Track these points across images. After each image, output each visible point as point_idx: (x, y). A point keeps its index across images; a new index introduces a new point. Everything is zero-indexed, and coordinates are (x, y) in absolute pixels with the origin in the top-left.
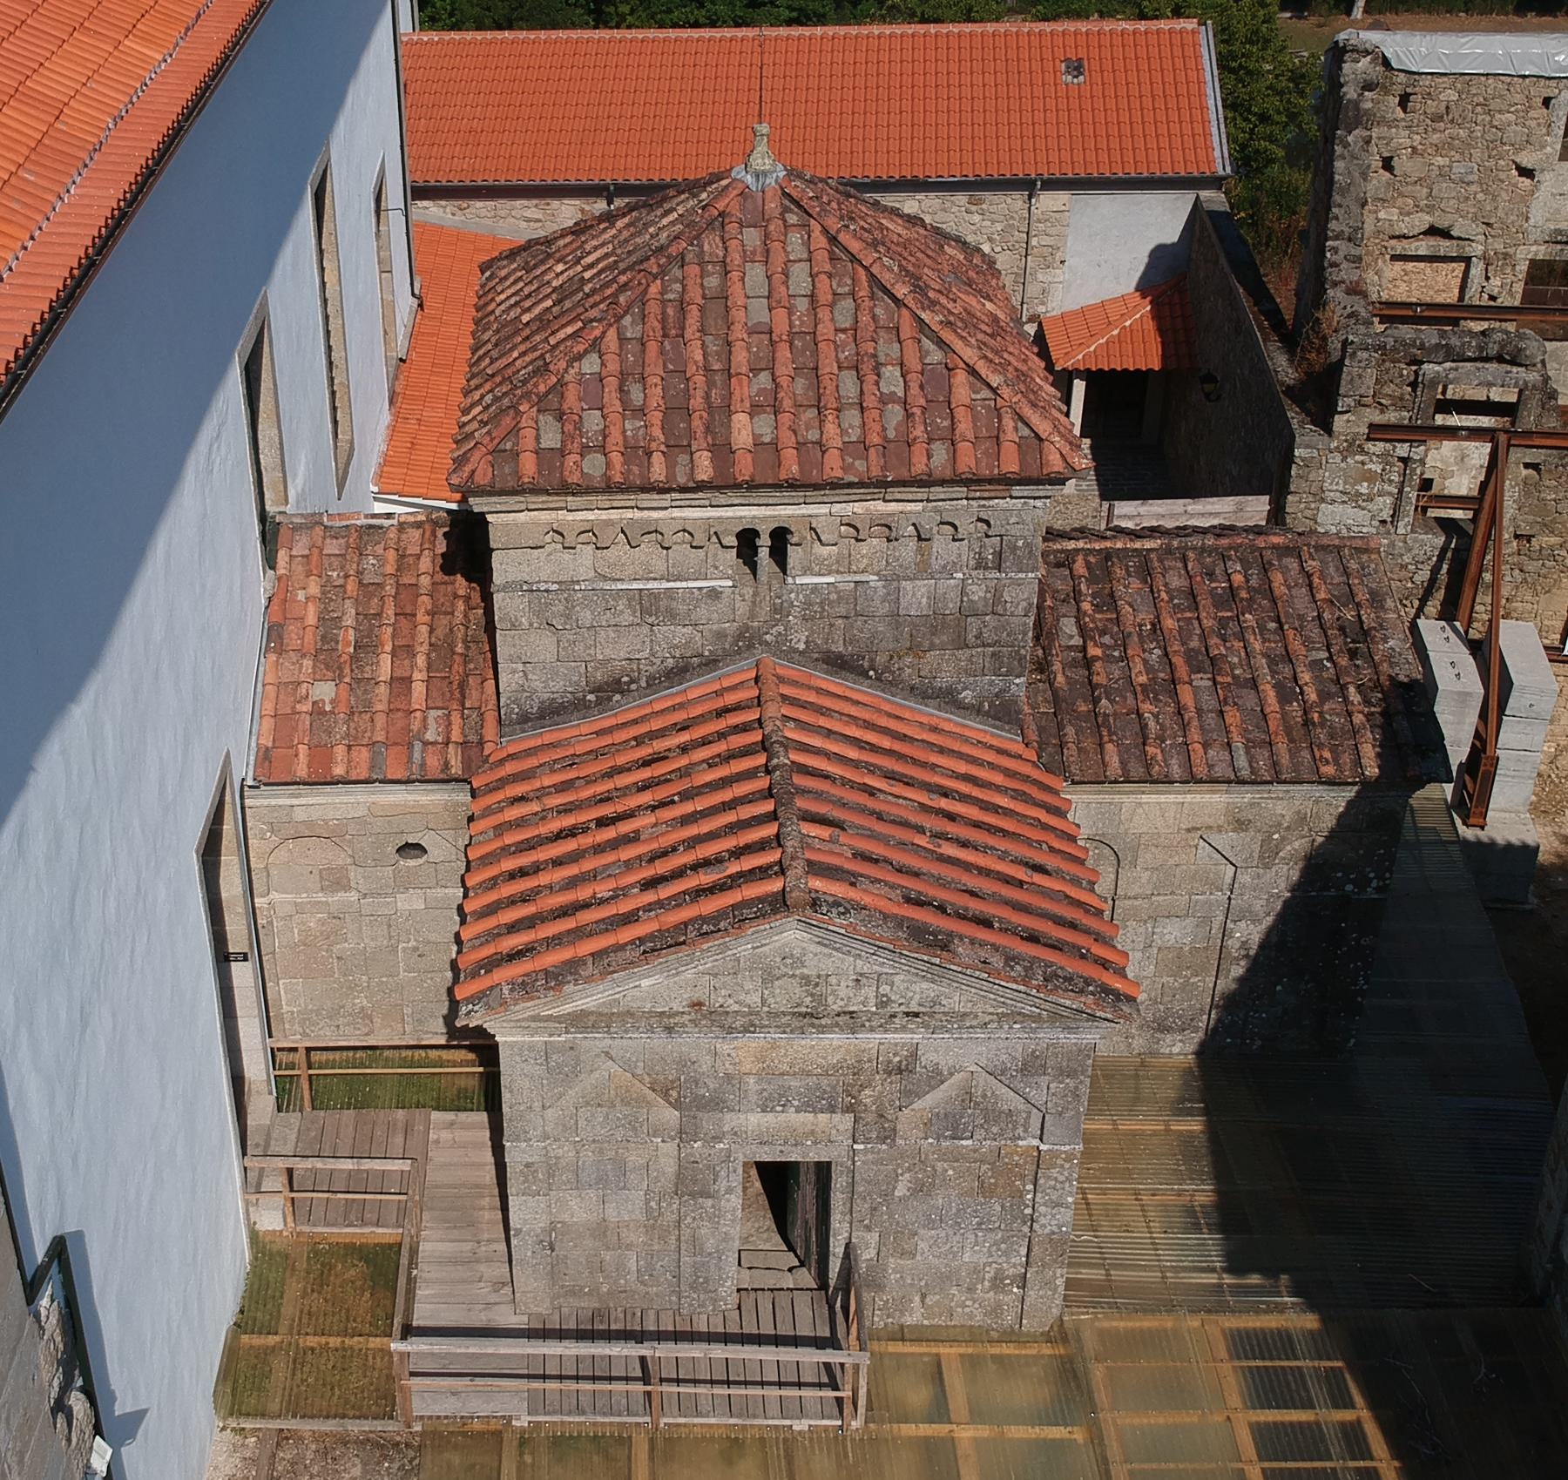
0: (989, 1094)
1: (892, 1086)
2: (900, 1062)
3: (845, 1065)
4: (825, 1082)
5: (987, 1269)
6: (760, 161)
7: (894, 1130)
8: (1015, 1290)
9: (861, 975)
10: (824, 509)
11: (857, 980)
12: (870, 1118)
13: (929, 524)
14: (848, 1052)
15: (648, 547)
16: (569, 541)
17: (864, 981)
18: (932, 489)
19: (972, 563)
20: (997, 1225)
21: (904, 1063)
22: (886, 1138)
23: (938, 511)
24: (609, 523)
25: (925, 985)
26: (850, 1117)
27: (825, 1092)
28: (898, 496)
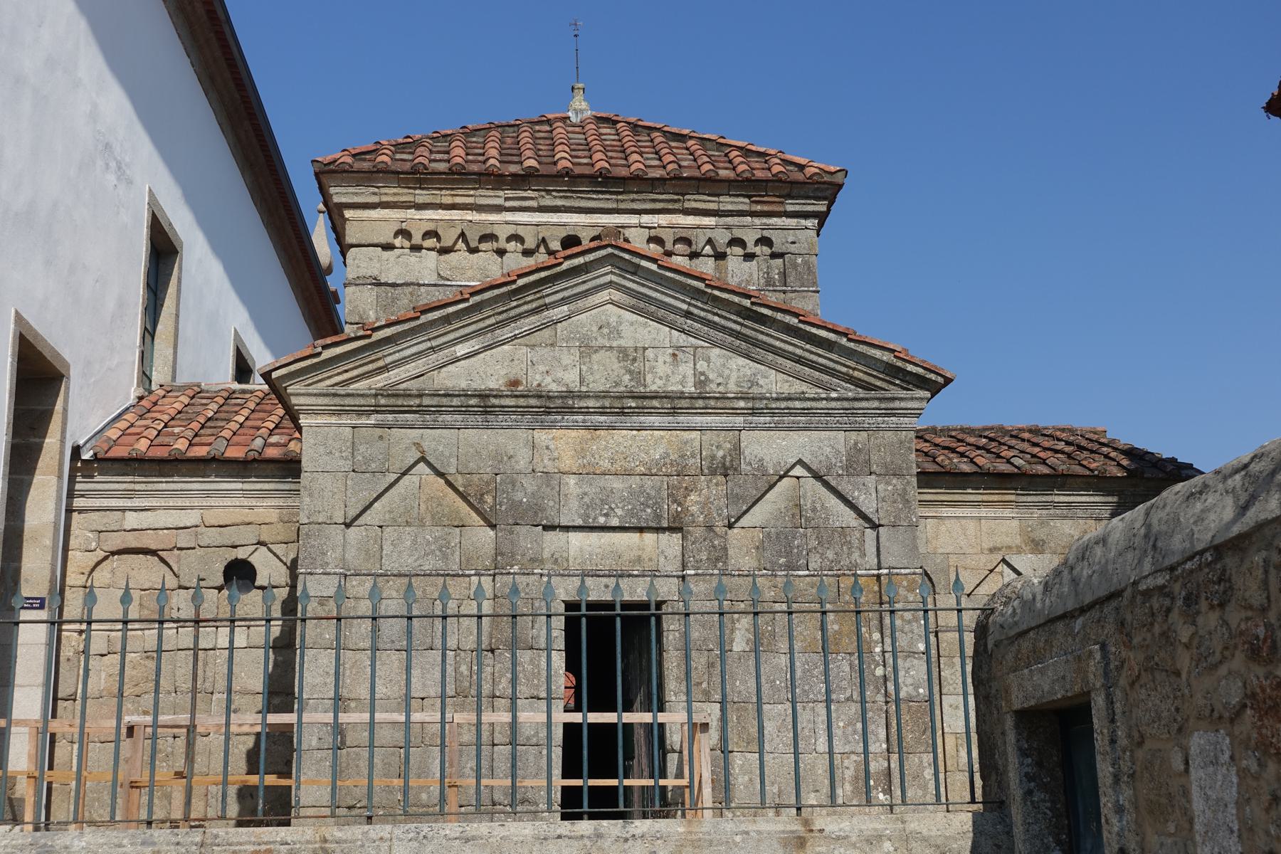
0: (818, 506)
2: (724, 457)
3: (669, 462)
4: (648, 482)
5: (846, 763)
6: (578, 103)
7: (725, 549)
8: (881, 796)
10: (633, 219)
11: (674, 355)
12: (698, 532)
13: (722, 238)
14: (669, 442)
16: (417, 239)
17: (680, 355)
18: (722, 198)
19: (762, 281)
20: (848, 695)
21: (728, 459)
22: (717, 560)
23: (728, 228)
25: (742, 361)
26: (677, 537)
27: (649, 497)
28: (694, 205)
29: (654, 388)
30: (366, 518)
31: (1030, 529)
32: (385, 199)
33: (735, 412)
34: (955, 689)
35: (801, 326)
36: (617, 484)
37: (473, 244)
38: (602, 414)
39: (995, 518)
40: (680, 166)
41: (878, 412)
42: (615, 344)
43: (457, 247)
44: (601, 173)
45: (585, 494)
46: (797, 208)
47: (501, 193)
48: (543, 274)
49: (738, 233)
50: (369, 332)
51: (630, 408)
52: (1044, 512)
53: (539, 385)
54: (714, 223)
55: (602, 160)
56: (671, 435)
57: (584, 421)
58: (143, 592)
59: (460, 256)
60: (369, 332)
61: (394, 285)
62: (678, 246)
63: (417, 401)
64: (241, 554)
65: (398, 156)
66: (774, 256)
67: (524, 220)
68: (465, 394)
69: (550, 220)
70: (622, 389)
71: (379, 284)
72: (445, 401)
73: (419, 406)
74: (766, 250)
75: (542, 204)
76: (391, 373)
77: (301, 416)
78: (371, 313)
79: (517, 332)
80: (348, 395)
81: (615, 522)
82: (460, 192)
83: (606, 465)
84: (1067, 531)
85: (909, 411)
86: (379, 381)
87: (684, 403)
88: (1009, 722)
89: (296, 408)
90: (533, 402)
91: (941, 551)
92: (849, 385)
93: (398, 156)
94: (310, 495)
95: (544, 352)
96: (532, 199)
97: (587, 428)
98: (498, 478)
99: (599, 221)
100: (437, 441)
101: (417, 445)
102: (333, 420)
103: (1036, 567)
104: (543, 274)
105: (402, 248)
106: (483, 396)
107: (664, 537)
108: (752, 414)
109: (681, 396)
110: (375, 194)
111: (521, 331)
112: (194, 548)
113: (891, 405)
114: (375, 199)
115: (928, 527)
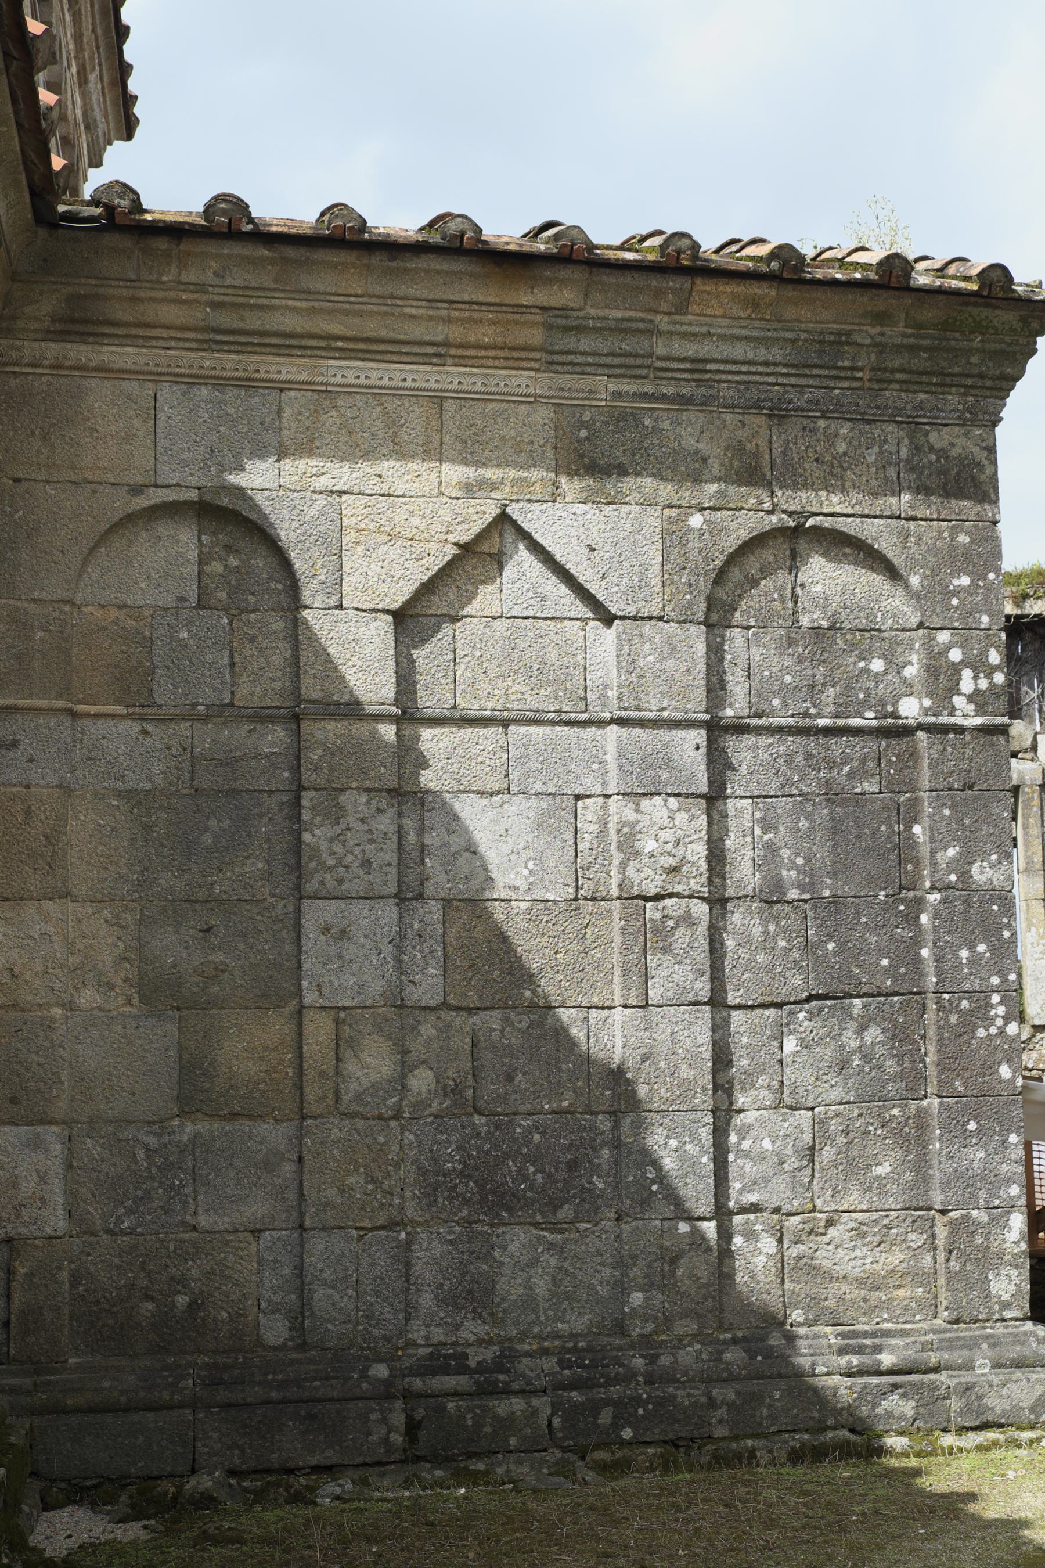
31: (583, 433)
34: (341, 881)
39: (485, 398)
52: (631, 387)
84: (690, 443)
103: (594, 539)
115: (287, 413)
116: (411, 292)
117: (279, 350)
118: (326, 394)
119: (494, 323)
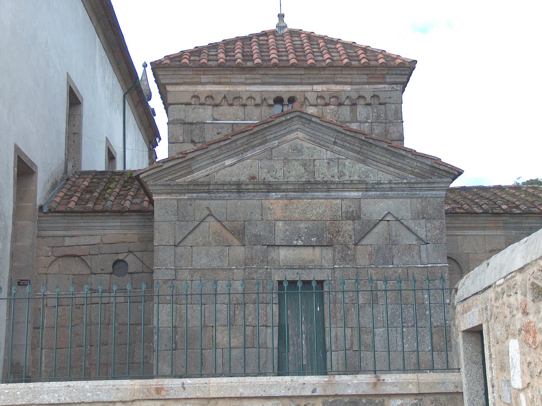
1: (348, 227)
2: (352, 212)
9: (330, 159)
10: (309, 88)
11: (329, 163)
13: (354, 95)
15: (237, 110)
16: (202, 100)
17: (332, 163)
24: (219, 92)
25: (361, 165)
28: (340, 80)
29: (318, 179)
30: (185, 243)
32: (186, 81)
33: (357, 190)
35: (389, 148)
36: (302, 225)
37: (230, 102)
38: (295, 192)
40: (333, 61)
41: (427, 189)
42: (300, 158)
43: (223, 104)
44: (293, 65)
45: (287, 230)
46: (392, 80)
47: (243, 76)
48: (266, 126)
49: (361, 93)
50: (184, 155)
51: (308, 189)
52: (518, 232)
53: (264, 178)
54: (349, 89)
55: (293, 58)
56: (327, 202)
57: (286, 195)
58: (74, 276)
59: (225, 109)
60: (184, 155)
61: (191, 124)
62: (332, 100)
63: (207, 187)
64: (121, 257)
65: (192, 58)
66: (380, 104)
67: (255, 89)
68: (230, 184)
69: (268, 89)
70: (304, 180)
71: (184, 124)
72: (220, 187)
73: (208, 190)
74: (376, 101)
75: (264, 81)
76: (195, 174)
77: (153, 195)
78: (181, 138)
79: (253, 153)
80: (175, 185)
81: (300, 243)
82: (224, 76)
83: (296, 216)
85: (442, 188)
86: (189, 178)
87: (332, 187)
88: (461, 335)
89: (151, 191)
90: (262, 187)
91: (465, 252)
92: (412, 176)
93: (192, 58)
94: (159, 233)
95: (267, 162)
96: (259, 79)
97: (287, 199)
98: (246, 223)
99: (293, 89)
100: (215, 205)
101: (208, 208)
102: (168, 197)
104: (266, 126)
105: (195, 104)
106: (238, 184)
107: (325, 250)
108: (367, 191)
109: (332, 183)
110: (181, 78)
111: (255, 153)
112: (98, 254)
113: (433, 186)
114: (182, 81)
116: (480, 219)
117: (457, 229)
118: (465, 235)
119: (494, 223)
